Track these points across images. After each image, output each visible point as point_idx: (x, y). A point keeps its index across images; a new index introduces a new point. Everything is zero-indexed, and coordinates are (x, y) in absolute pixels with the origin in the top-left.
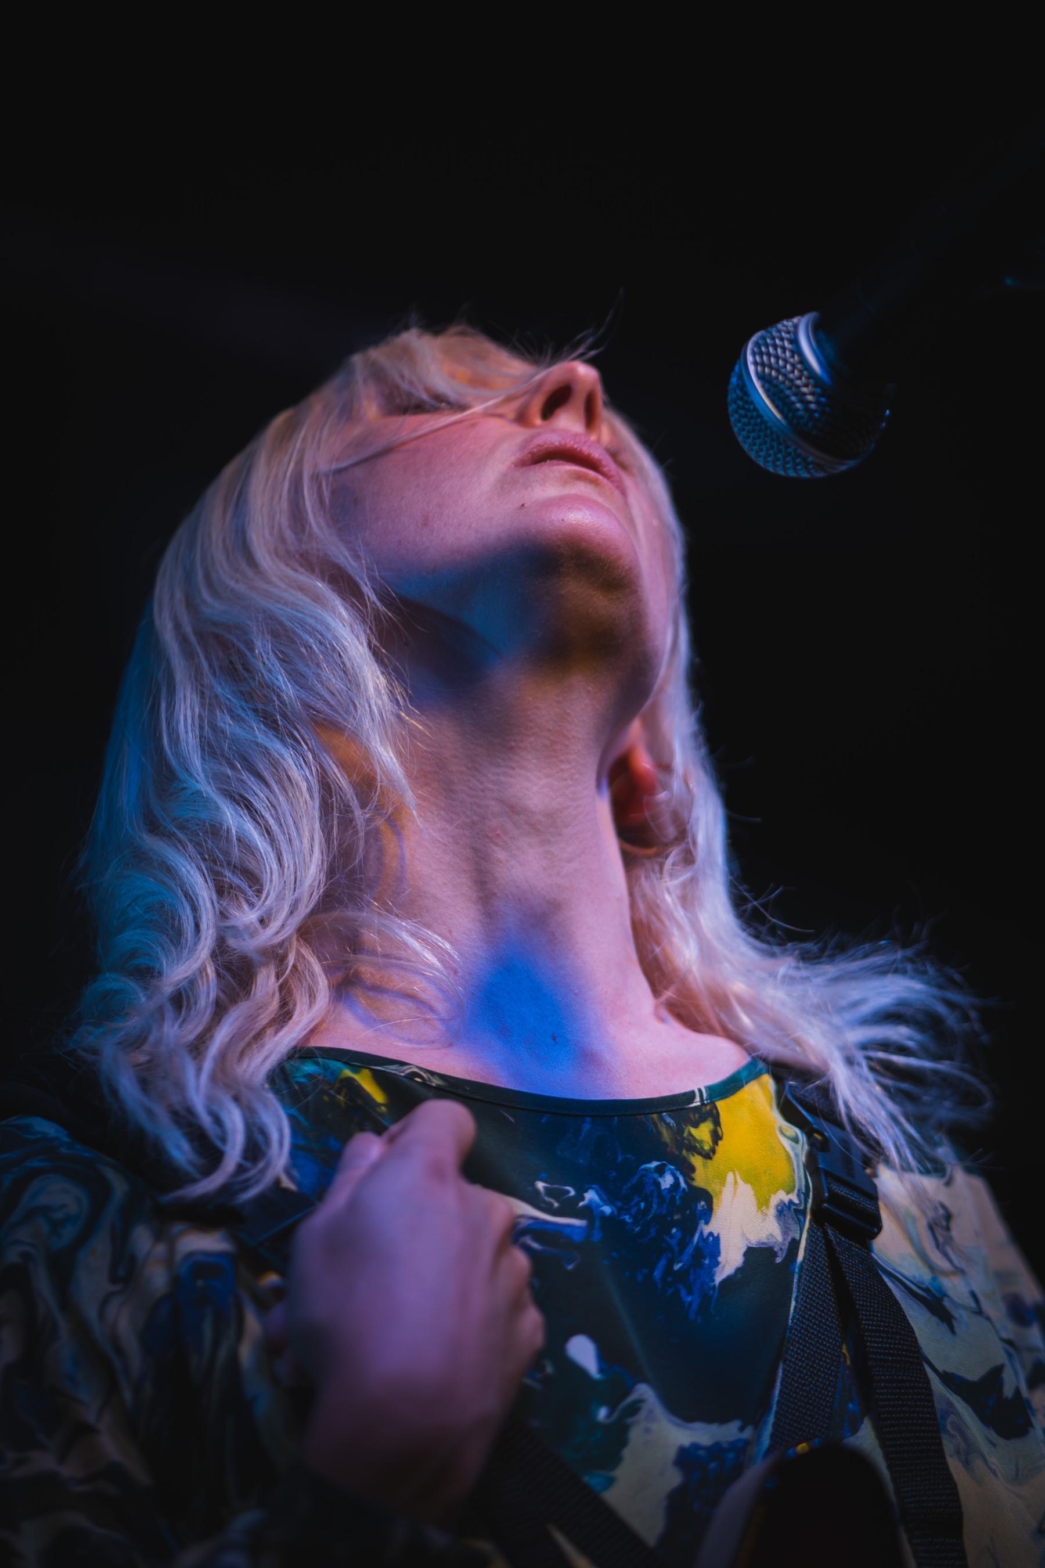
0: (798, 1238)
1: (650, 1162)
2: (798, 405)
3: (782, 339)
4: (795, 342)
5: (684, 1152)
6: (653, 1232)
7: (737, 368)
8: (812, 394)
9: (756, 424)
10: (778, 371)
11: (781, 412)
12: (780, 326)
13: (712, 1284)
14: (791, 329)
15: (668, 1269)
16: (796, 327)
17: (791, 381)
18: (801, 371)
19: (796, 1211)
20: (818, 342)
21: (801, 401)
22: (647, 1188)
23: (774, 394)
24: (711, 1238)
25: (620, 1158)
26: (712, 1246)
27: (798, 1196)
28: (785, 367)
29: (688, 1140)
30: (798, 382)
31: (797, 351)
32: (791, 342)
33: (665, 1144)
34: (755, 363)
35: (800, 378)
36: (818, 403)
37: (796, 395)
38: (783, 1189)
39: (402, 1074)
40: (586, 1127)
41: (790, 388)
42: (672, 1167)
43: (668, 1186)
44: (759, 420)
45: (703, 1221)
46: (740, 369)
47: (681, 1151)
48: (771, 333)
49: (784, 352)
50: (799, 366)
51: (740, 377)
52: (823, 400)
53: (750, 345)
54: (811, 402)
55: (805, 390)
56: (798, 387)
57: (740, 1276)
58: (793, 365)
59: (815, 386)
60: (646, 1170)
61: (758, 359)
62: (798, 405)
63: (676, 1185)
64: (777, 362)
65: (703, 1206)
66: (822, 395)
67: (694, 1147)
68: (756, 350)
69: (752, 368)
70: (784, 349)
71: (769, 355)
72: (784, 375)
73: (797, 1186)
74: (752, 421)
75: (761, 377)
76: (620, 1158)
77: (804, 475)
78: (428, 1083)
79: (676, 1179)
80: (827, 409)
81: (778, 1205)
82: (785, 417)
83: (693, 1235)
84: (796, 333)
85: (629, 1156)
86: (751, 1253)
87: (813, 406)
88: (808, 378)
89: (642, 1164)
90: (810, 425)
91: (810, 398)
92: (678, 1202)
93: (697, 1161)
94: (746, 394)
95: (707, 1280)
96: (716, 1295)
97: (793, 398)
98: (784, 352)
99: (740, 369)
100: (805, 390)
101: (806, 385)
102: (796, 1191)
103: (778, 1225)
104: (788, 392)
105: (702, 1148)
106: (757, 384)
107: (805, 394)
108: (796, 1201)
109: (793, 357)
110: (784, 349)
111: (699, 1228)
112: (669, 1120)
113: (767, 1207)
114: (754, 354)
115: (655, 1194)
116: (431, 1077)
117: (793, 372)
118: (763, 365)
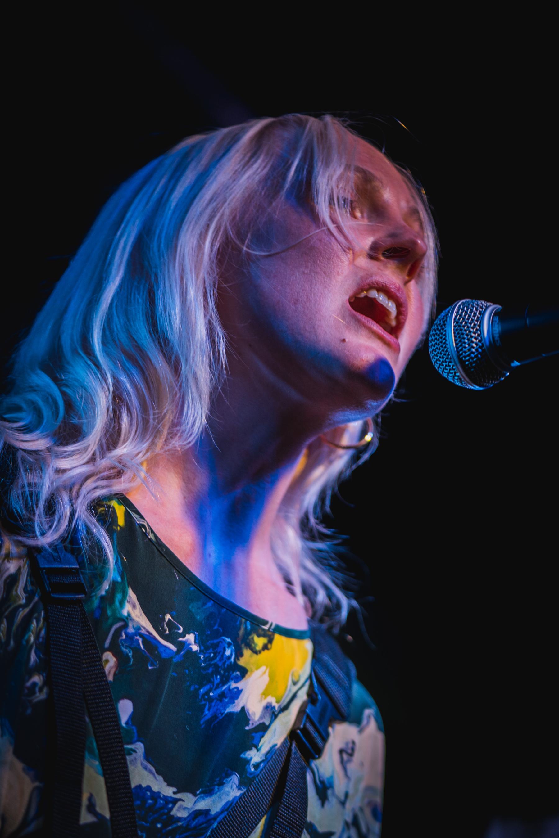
2: (467, 346)
3: (477, 309)
4: (482, 314)
6: (211, 670)
8: (476, 344)
10: (466, 323)
12: (479, 302)
15: (207, 693)
17: (470, 332)
18: (477, 330)
21: (469, 345)
22: (217, 649)
28: (471, 324)
30: (473, 335)
31: (481, 320)
32: (480, 313)
35: (475, 333)
36: (477, 350)
37: (468, 340)
41: (467, 335)
42: (233, 648)
43: (227, 655)
47: (242, 644)
48: (473, 303)
49: (474, 316)
50: (478, 328)
52: (480, 350)
54: (473, 347)
55: (474, 340)
56: (472, 337)
58: (475, 325)
59: (480, 341)
62: (467, 346)
63: (229, 657)
64: (468, 319)
66: (480, 347)
69: (454, 314)
70: (475, 314)
71: (466, 312)
72: (468, 327)
79: (231, 654)
80: (479, 356)
84: (485, 310)
87: (473, 350)
88: (479, 335)
90: (467, 358)
91: (474, 345)
92: (226, 666)
93: (247, 653)
97: (466, 341)
98: (474, 316)
100: (474, 340)
101: (476, 339)
104: (465, 336)
107: (473, 342)
109: (477, 321)
110: (475, 314)
115: (221, 653)
117: (473, 328)
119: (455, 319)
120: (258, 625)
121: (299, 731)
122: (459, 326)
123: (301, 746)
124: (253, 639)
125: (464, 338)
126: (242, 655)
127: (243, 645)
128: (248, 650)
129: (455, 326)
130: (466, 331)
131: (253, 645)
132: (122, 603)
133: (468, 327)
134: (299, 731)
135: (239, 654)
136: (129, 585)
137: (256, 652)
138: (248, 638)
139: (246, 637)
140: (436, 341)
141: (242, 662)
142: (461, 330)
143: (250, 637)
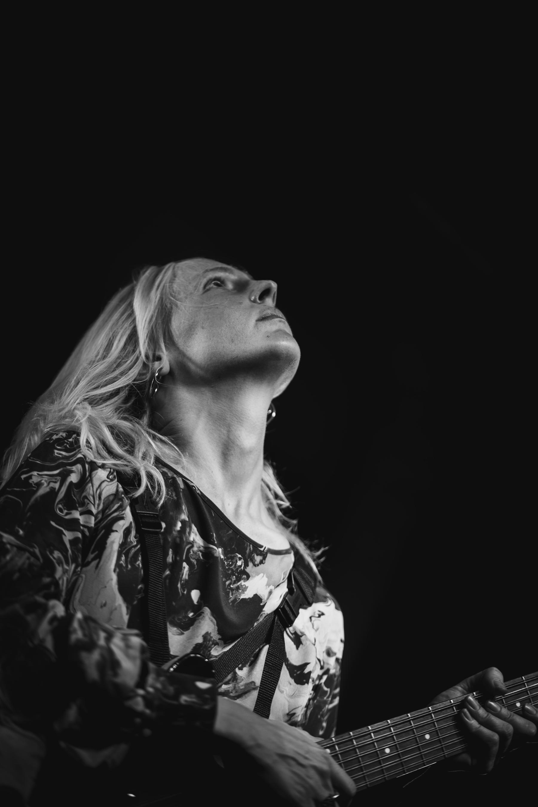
1: (239, 554)
5: (249, 559)
13: (239, 597)
24: (244, 586)
25: (233, 547)
29: (252, 557)
33: (246, 553)
40: (230, 532)
47: (248, 558)
57: (249, 600)
60: (237, 555)
67: (253, 560)
76: (233, 547)
85: (236, 548)
86: (256, 596)
89: (237, 553)
93: (251, 564)
95: (238, 595)
96: (239, 601)
105: (255, 562)
112: (251, 547)
120: (257, 548)
121: (280, 610)
123: (280, 618)
124: (254, 556)
126: (248, 566)
127: (249, 559)
128: (251, 563)
131: (254, 561)
132: (189, 533)
134: (280, 610)
135: (246, 565)
136: (193, 522)
137: (255, 565)
138: (251, 556)
139: (250, 555)
141: (248, 570)
143: (253, 555)
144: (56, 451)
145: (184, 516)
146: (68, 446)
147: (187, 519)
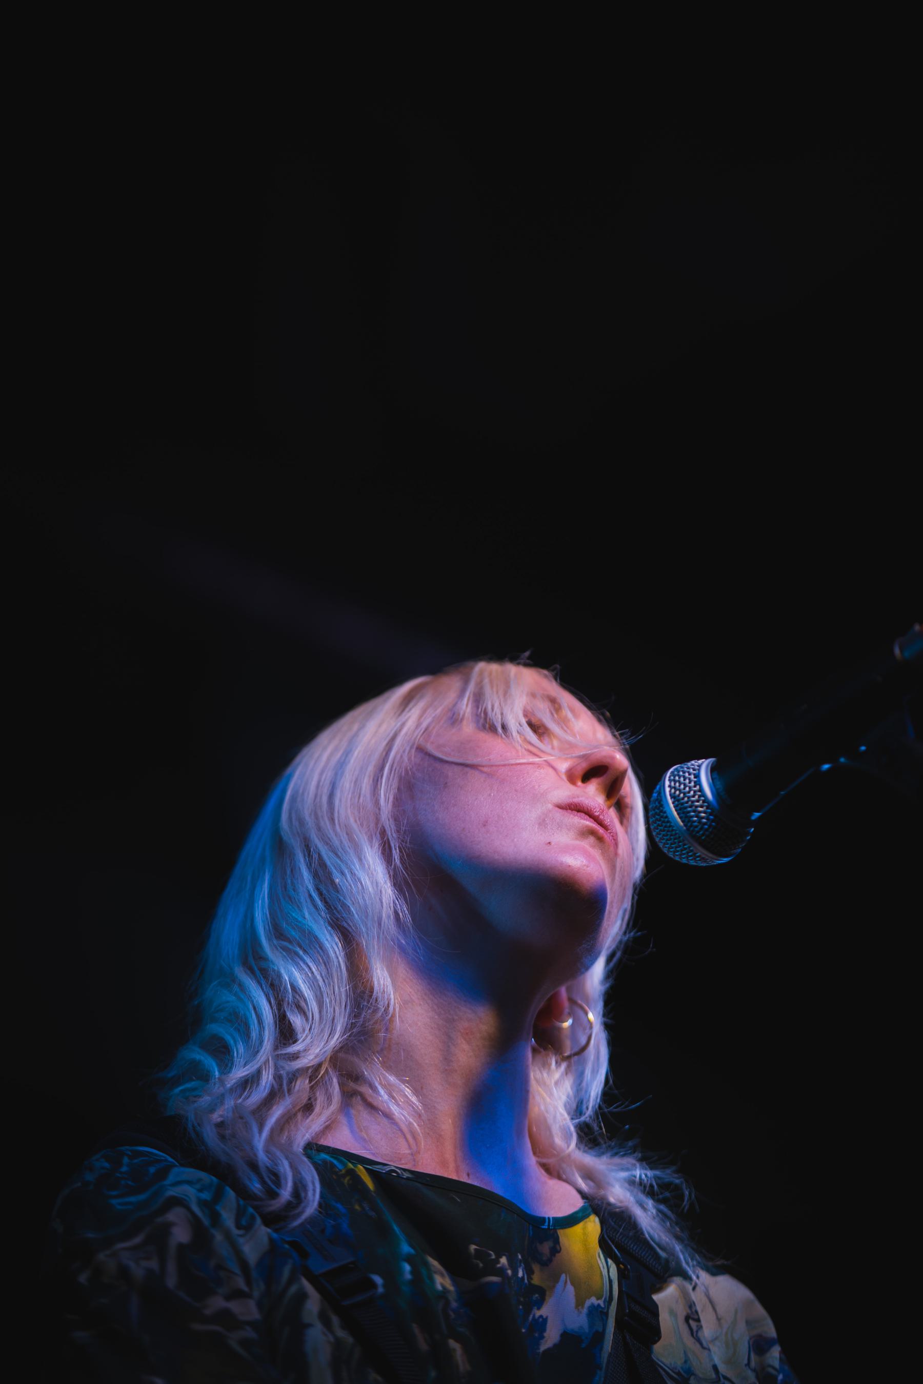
0: (600, 1330)
7: (658, 787)
9: (665, 827)
10: (684, 794)
11: (683, 822)
14: (696, 767)
16: (699, 766)
18: (699, 796)
19: (601, 1312)
20: (713, 779)
23: (680, 809)
26: (541, 1324)
27: (604, 1302)
34: (670, 786)
38: (596, 1296)
39: (384, 1171)
44: (668, 824)
45: (536, 1308)
46: (660, 788)
50: (699, 793)
51: (659, 793)
53: (669, 774)
61: (673, 784)
65: (537, 1297)
68: (672, 778)
73: (604, 1296)
74: (664, 824)
75: (672, 796)
77: (692, 863)
78: (401, 1176)
81: (589, 1307)
82: (685, 825)
83: (529, 1316)
88: (704, 802)
94: (662, 806)
99: (660, 788)
101: (702, 807)
102: (603, 1299)
103: (587, 1321)
106: (670, 801)
108: (602, 1305)
111: (533, 1312)
113: (583, 1307)
114: (670, 780)
116: (404, 1173)
118: (675, 788)
119: (670, 795)
122: (678, 801)
125: (689, 812)
129: (673, 803)
130: (687, 802)
133: (689, 798)
140: (658, 822)
142: (682, 804)
144: (114, 1202)
145: (406, 1248)
146: (130, 1183)
147: (412, 1251)
